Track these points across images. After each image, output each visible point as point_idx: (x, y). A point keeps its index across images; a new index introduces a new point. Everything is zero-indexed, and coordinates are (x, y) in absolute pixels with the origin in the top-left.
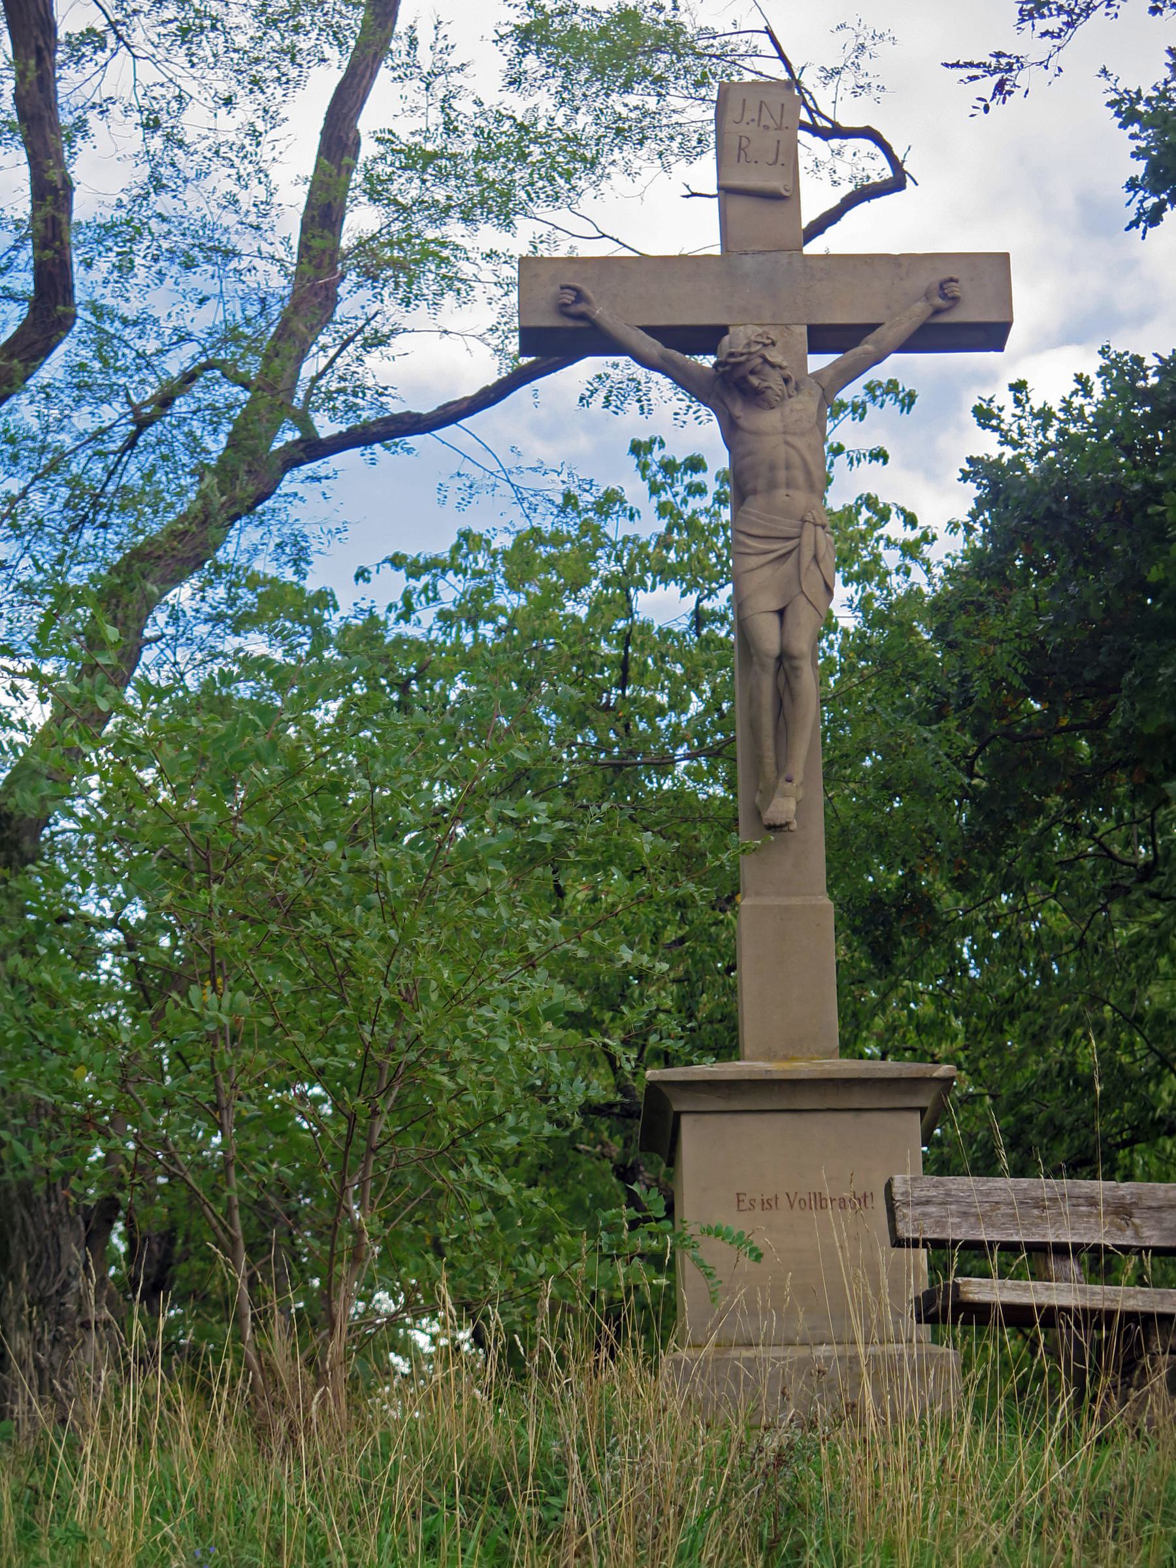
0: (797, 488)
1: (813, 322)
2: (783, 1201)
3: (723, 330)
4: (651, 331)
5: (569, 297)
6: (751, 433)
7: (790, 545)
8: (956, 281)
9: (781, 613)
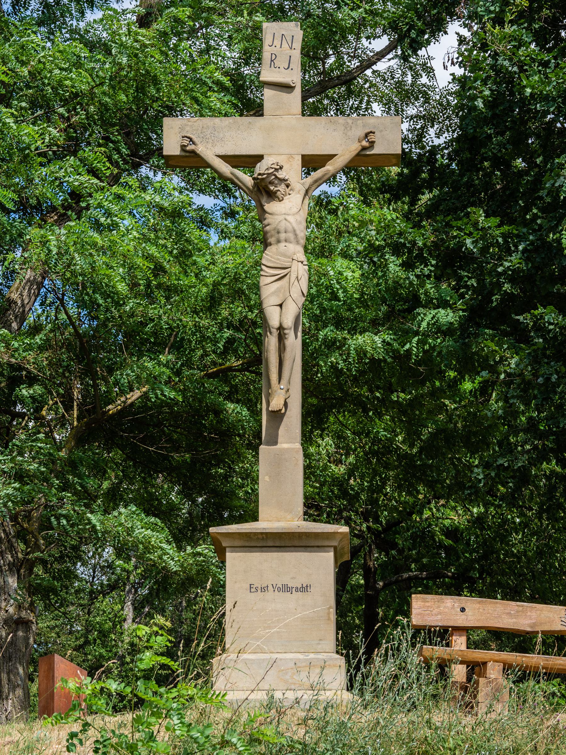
0: (290, 242)
1: (304, 153)
2: (270, 587)
3: (260, 158)
4: (225, 158)
5: (186, 142)
6: (270, 214)
7: (286, 271)
8: (374, 133)
9: (281, 306)
